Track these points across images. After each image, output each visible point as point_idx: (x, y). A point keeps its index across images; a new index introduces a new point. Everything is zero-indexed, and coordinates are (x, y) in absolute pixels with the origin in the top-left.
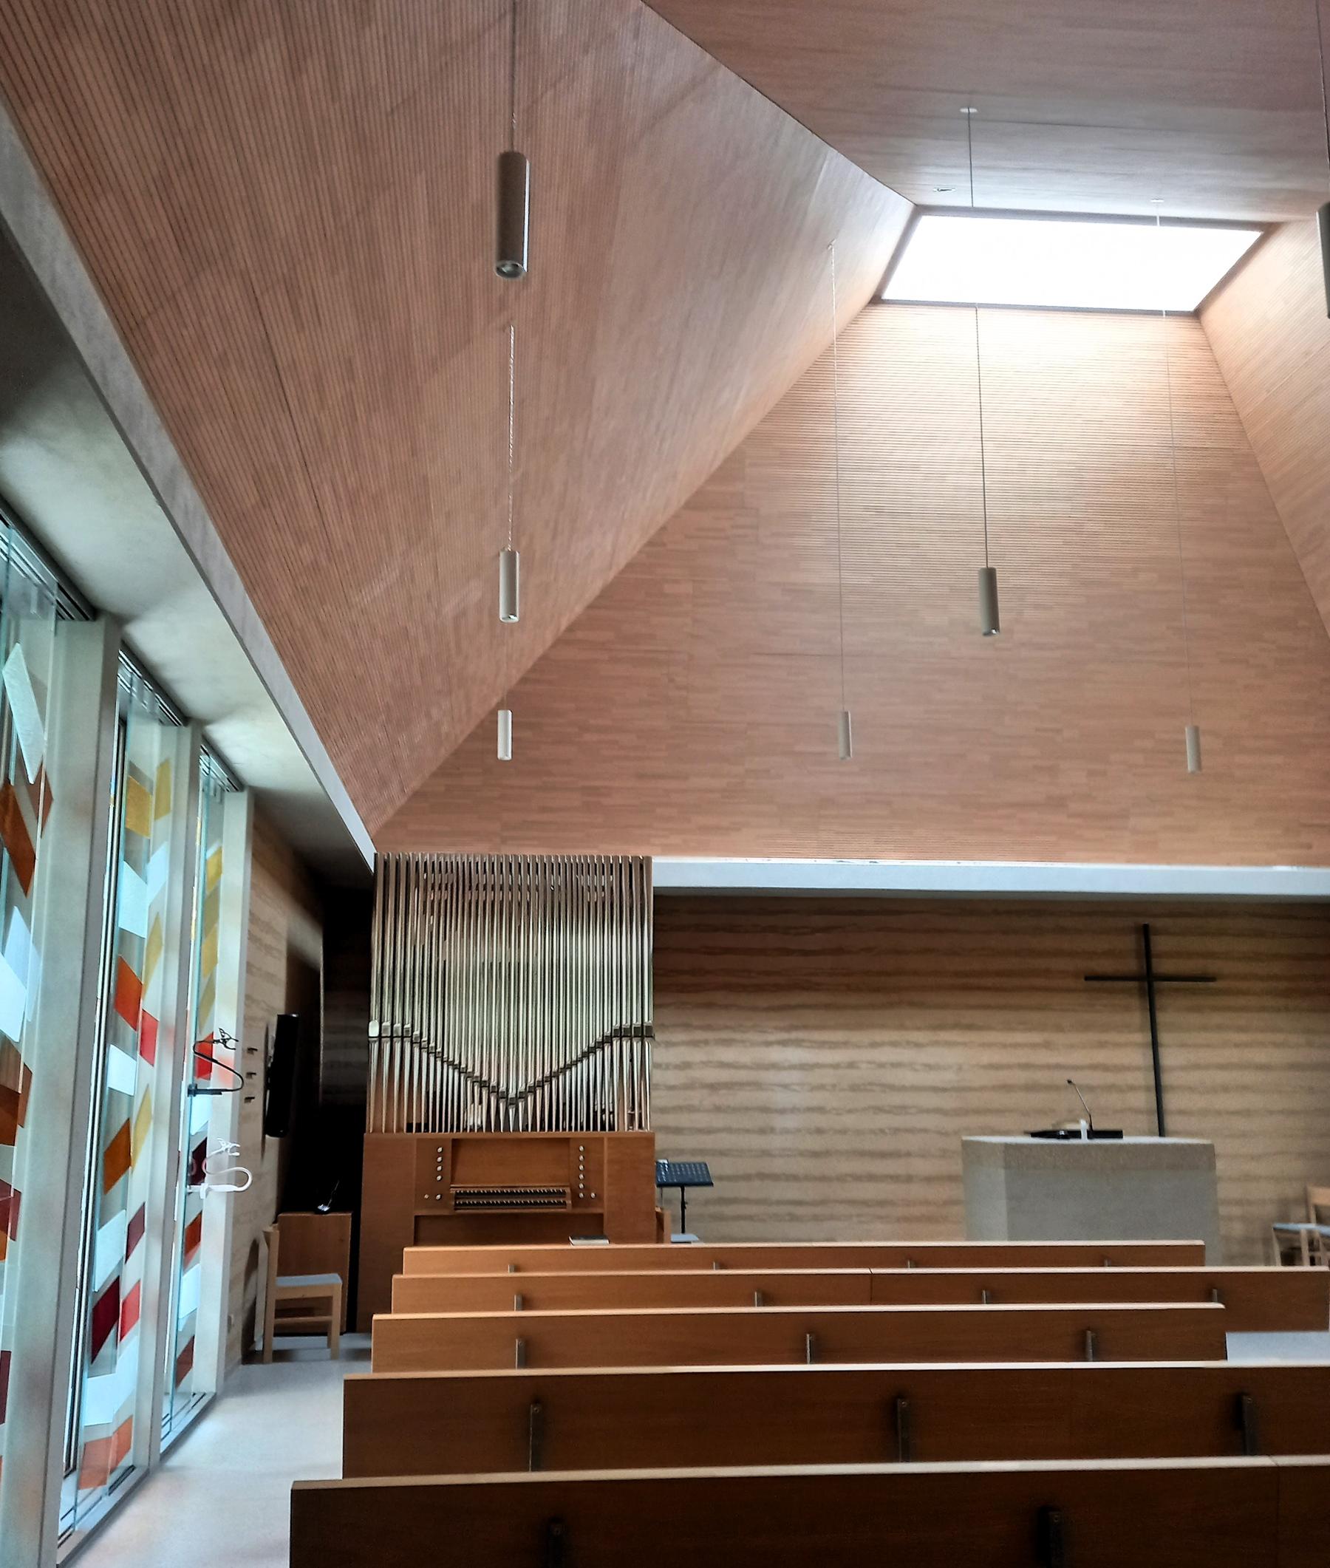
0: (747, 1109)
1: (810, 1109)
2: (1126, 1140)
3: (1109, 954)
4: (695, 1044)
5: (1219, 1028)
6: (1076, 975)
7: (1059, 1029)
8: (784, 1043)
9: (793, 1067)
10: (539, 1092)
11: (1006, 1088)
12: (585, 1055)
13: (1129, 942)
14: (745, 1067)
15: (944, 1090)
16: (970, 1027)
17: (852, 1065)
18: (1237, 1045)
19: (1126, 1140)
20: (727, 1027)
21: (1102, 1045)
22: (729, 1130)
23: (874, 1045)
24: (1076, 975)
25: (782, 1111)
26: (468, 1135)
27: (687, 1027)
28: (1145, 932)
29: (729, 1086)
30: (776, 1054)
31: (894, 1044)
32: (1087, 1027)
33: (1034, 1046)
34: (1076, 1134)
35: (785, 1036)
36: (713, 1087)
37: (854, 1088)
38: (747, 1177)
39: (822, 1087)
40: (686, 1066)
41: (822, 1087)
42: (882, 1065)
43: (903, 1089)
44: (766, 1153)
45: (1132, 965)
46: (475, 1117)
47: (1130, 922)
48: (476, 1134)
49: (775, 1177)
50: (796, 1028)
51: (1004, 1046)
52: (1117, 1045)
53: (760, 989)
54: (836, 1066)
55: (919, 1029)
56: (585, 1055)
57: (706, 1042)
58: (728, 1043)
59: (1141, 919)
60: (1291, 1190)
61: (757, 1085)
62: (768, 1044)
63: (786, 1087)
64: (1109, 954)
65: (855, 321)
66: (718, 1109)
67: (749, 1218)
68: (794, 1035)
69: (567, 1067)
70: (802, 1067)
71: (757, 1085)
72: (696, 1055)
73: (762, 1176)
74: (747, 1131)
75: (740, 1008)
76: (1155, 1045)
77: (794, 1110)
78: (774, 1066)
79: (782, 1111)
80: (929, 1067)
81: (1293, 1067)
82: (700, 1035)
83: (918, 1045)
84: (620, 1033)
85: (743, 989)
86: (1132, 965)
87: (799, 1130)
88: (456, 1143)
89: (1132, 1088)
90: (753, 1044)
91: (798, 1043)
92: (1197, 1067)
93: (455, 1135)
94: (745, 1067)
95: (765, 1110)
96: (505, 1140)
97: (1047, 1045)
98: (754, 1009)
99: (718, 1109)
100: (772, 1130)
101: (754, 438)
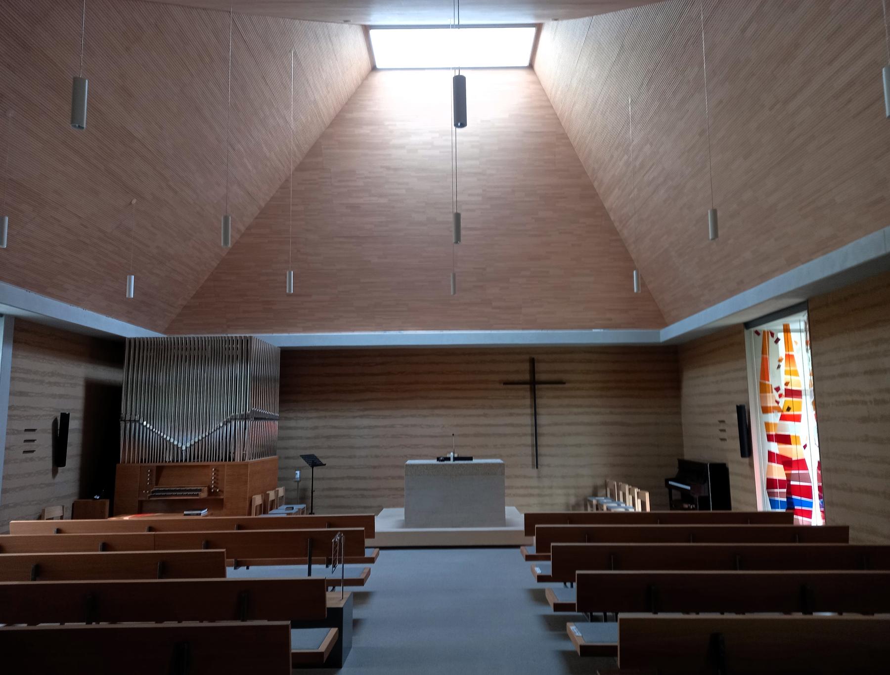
1: (372, 447)
2: (475, 461)
3: (517, 372)
4: (319, 418)
5: (568, 406)
6: (500, 382)
7: (491, 407)
8: (361, 417)
9: (365, 428)
11: (465, 435)
13: (526, 366)
15: (436, 437)
16: (449, 407)
17: (392, 426)
18: (575, 414)
19: (475, 461)
21: (511, 415)
23: (403, 417)
24: (500, 382)
25: (359, 448)
27: (317, 410)
28: (532, 362)
29: (336, 437)
30: (358, 422)
31: (412, 416)
32: (504, 407)
33: (479, 416)
34: (449, 459)
35: (361, 413)
36: (328, 437)
37: (393, 436)
38: (343, 478)
39: (377, 436)
40: (316, 428)
41: (377, 436)
42: (406, 426)
43: (416, 436)
44: (351, 467)
45: (527, 377)
47: (527, 357)
49: (356, 478)
50: (366, 410)
51: (465, 416)
52: (518, 415)
54: (385, 427)
55: (425, 408)
57: (325, 417)
58: (336, 417)
59: (531, 356)
60: (600, 482)
61: (349, 436)
62: (354, 417)
63: (361, 437)
64: (517, 372)
65: (366, 78)
66: (330, 447)
67: (343, 497)
68: (366, 413)
70: (370, 427)
71: (349, 436)
72: (321, 423)
73: (349, 478)
76: (535, 414)
77: (365, 447)
78: (356, 427)
79: (359, 448)
80: (429, 426)
81: (604, 423)
82: (323, 414)
83: (425, 416)
86: (527, 377)
87: (367, 457)
89: (525, 435)
91: (367, 416)
92: (556, 424)
95: (352, 447)
96: (175, 467)
97: (485, 415)
99: (330, 447)
100: (355, 457)
101: (324, 136)
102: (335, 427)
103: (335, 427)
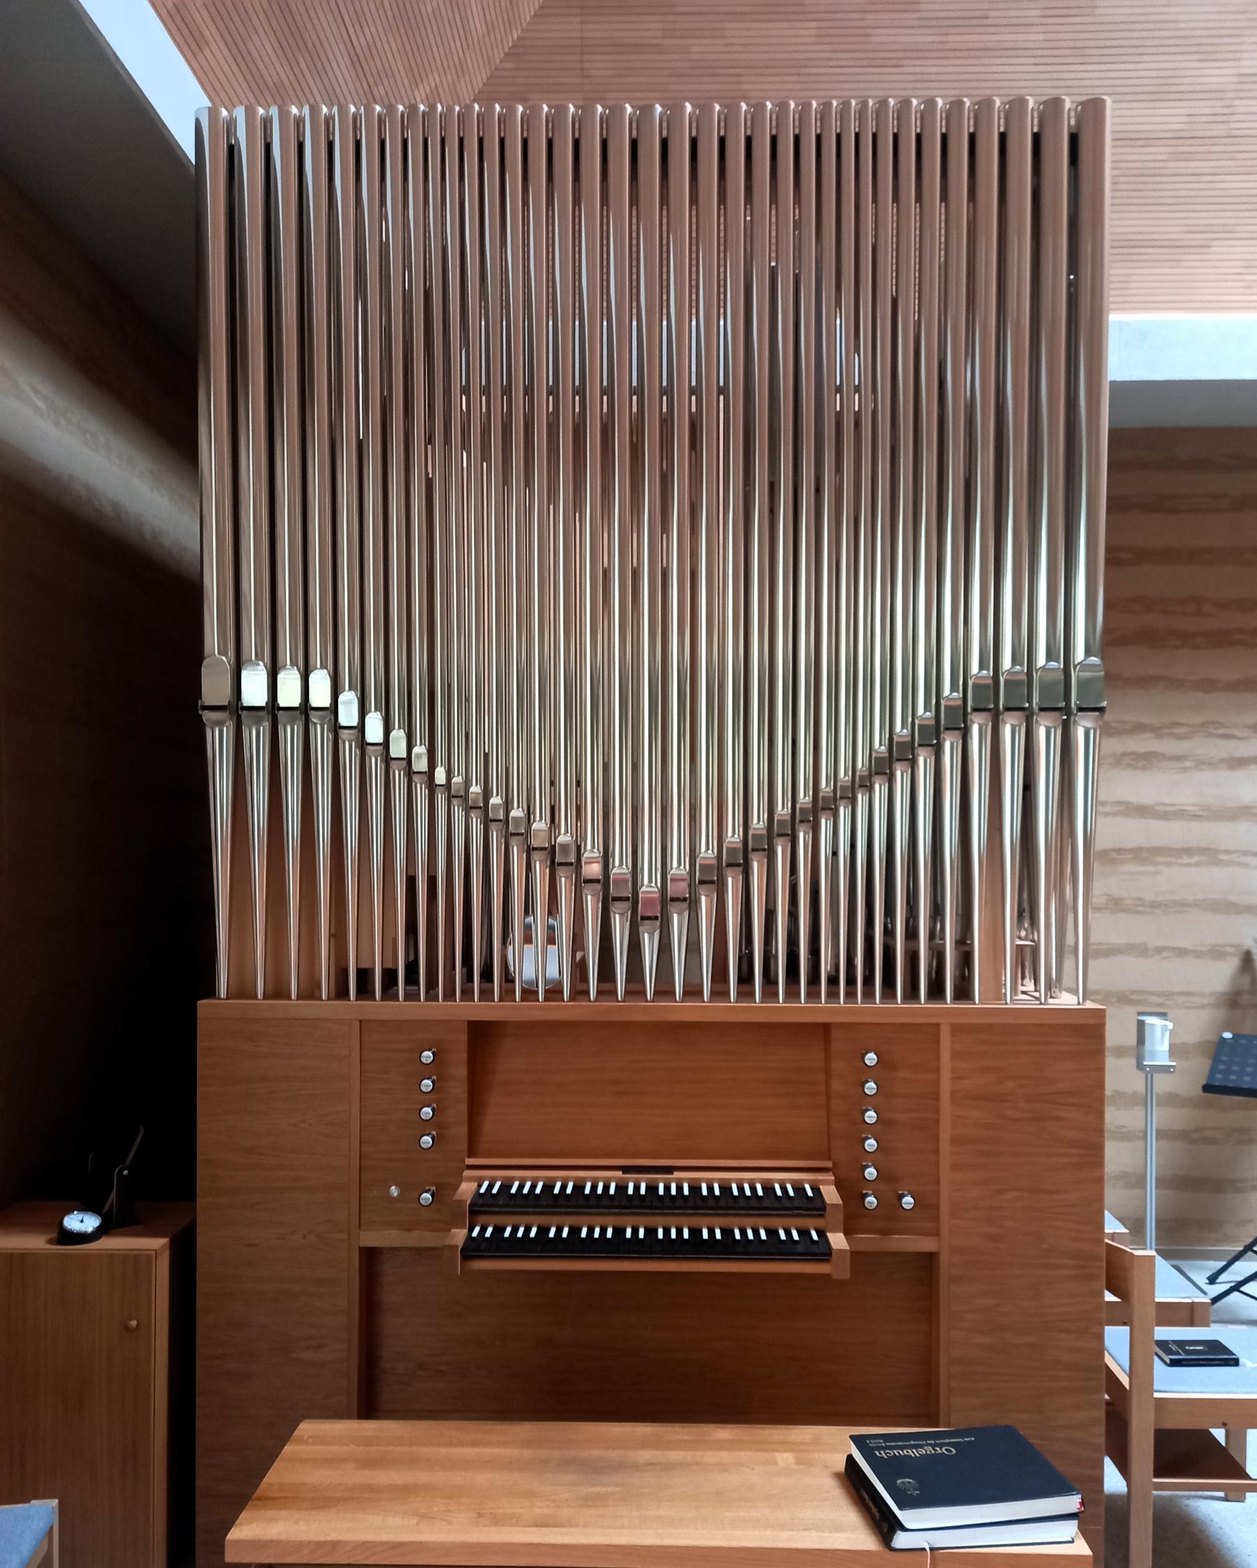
0: (1182, 906)
10: (732, 884)
12: (882, 768)
14: (1181, 814)
20: (1140, 728)
22: (1139, 950)
26: (516, 1010)
46: (538, 962)
48: (540, 1010)
53: (1220, 640)
56: (882, 768)
58: (1146, 760)
61: (1210, 855)
69: (823, 806)
71: (1210, 855)
74: (1181, 952)
75: (1176, 684)
84: (993, 699)
85: (1185, 639)
88: (482, 1035)
90: (1204, 764)
93: (478, 1009)
94: (1181, 814)
98: (1209, 686)
102: (1142, 811)
103: (1142, 811)
